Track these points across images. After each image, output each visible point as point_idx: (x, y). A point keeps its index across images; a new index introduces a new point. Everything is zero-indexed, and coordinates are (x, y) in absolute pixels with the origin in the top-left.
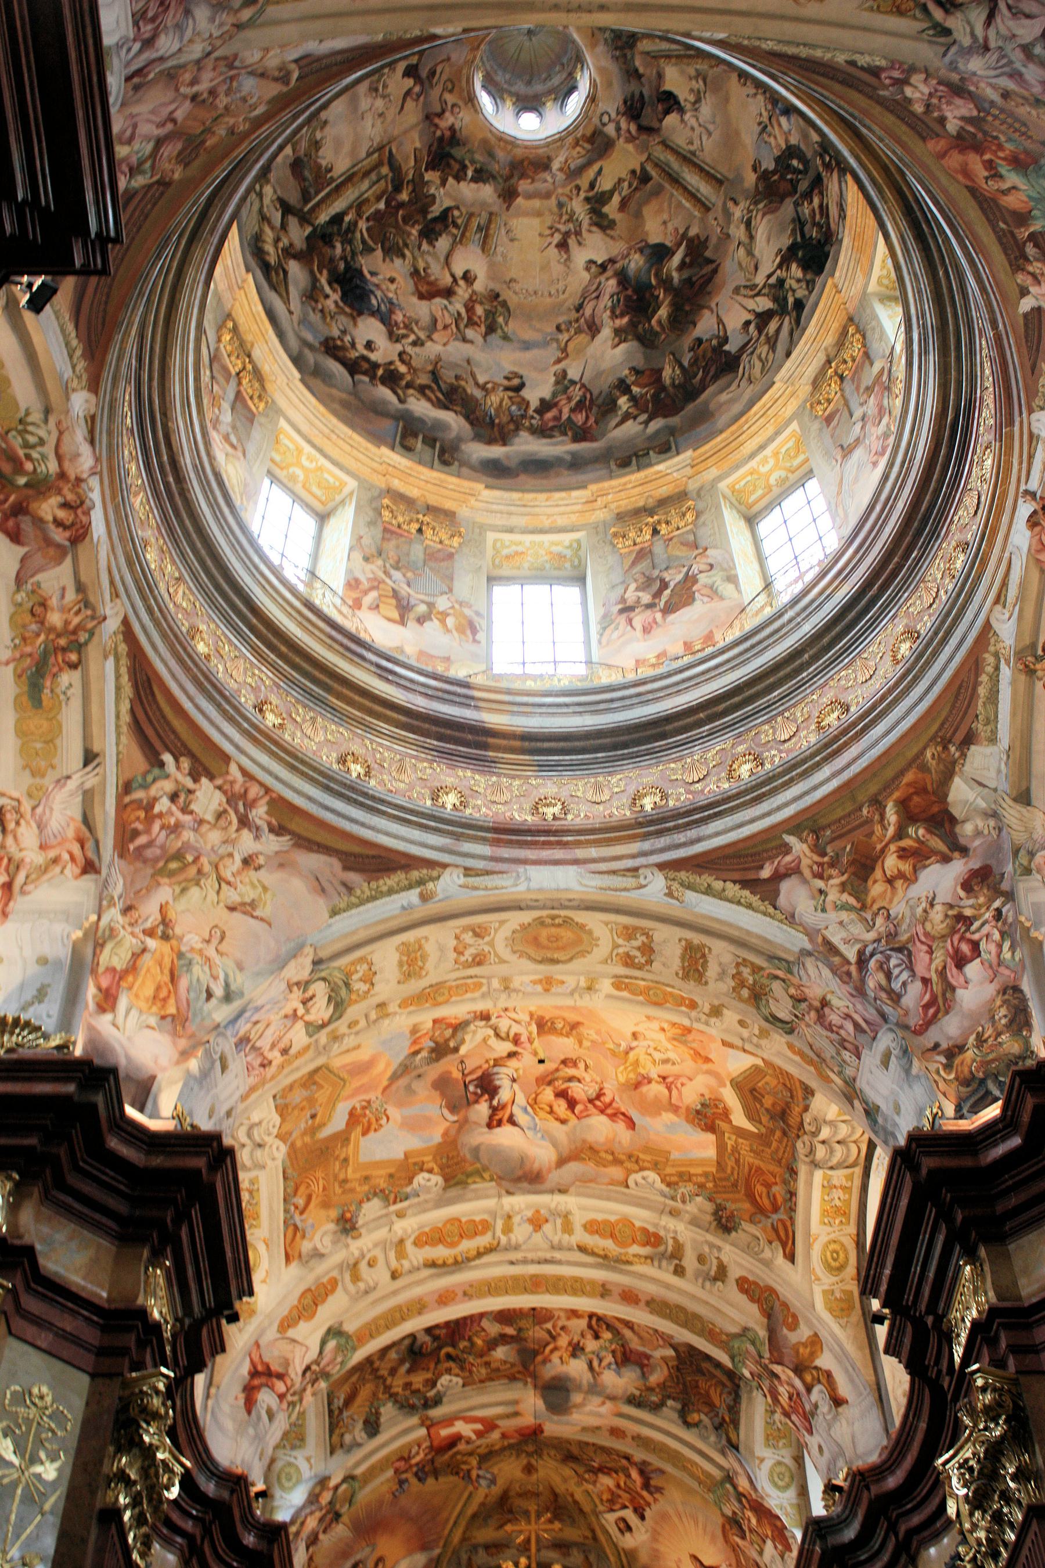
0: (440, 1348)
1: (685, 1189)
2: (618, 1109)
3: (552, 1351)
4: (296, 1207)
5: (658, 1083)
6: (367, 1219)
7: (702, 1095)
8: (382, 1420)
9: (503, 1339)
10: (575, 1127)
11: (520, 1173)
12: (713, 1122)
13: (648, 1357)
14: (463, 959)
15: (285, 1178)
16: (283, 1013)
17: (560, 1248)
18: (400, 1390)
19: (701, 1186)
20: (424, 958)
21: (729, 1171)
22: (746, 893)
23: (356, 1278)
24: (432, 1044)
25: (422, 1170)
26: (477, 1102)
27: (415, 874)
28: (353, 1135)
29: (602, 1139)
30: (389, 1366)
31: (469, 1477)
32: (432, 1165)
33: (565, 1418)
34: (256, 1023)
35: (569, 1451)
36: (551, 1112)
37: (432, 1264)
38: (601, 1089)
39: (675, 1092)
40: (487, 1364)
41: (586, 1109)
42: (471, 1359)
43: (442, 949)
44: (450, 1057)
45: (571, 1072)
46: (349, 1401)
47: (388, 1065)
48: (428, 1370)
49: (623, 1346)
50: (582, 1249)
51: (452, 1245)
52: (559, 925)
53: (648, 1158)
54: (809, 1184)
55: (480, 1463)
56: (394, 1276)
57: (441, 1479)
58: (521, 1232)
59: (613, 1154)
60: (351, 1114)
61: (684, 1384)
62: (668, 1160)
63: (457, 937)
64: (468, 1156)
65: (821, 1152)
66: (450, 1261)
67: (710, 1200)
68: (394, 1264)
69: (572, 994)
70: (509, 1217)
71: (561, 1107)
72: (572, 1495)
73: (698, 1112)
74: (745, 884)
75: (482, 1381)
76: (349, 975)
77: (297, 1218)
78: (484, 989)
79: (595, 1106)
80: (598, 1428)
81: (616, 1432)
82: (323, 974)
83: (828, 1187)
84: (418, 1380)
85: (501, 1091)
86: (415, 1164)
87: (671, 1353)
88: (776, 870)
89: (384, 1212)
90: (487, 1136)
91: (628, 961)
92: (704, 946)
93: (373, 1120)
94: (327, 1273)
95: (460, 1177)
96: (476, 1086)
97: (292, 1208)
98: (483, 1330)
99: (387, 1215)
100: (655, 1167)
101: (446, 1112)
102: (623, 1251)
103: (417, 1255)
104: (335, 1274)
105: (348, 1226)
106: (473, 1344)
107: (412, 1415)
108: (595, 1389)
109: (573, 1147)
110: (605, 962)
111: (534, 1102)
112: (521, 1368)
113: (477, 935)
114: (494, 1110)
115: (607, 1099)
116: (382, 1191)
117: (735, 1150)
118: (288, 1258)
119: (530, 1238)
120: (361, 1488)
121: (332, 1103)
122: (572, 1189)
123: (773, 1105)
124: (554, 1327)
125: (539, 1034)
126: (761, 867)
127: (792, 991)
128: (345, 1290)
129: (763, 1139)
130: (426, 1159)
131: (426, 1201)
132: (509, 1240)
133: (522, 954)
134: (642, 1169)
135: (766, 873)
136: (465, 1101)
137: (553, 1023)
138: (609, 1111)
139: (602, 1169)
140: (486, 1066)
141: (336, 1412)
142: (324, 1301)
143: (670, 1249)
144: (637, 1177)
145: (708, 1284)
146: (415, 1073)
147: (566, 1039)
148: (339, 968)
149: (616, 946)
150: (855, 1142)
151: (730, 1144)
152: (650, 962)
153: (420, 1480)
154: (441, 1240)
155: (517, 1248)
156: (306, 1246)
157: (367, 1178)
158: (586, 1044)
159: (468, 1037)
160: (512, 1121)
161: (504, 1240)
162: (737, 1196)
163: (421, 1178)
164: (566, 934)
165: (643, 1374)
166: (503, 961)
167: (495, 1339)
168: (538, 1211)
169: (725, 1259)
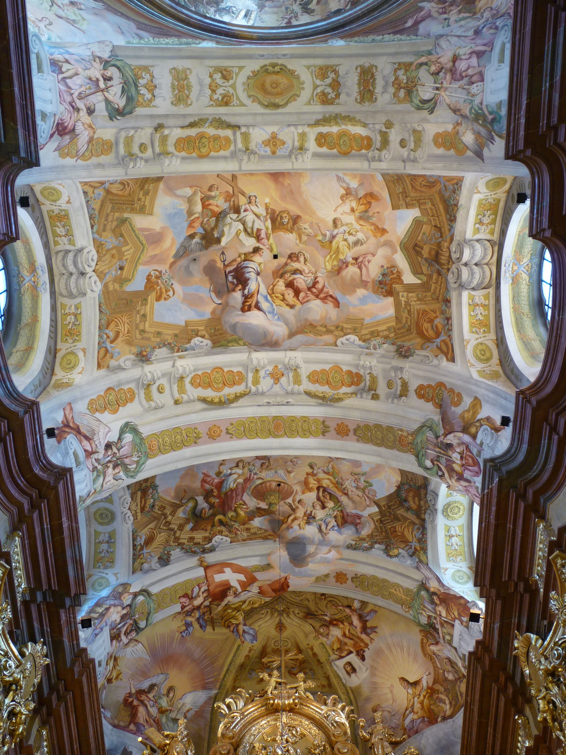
0: (214, 515)
1: (375, 341)
2: (327, 293)
3: (293, 521)
4: (108, 337)
5: (353, 264)
6: (157, 357)
7: (382, 267)
8: (172, 558)
9: (259, 512)
10: (300, 310)
11: (264, 342)
12: (391, 288)
13: (359, 517)
14: (215, 97)
15: (100, 311)
16: (88, 73)
17: (292, 393)
18: (185, 541)
19: (386, 337)
20: (189, 87)
21: (404, 321)
22: (398, 36)
23: (149, 398)
25: (197, 335)
26: (234, 290)
27: (184, 40)
29: (318, 318)
30: (178, 522)
31: (238, 631)
32: (203, 333)
33: (303, 569)
34: (67, 61)
35: (308, 608)
36: (284, 300)
37: (204, 400)
38: (316, 278)
40: (248, 529)
41: (307, 296)
42: (236, 525)
43: (201, 84)
44: (215, 247)
45: (296, 265)
46: (149, 541)
47: (173, 243)
48: (206, 530)
49: (342, 511)
50: (308, 393)
51: (218, 390)
52: (278, 73)
53: (349, 326)
54: (460, 304)
55: (245, 619)
56: (177, 402)
57: (217, 630)
58: (266, 384)
59: (326, 326)
60: (149, 277)
61: (386, 531)
62: (362, 325)
63: (211, 76)
64: (229, 330)
65: (465, 274)
66: (216, 400)
67: (393, 344)
68: (177, 396)
69: (290, 156)
70: (257, 371)
71: (290, 295)
72: (312, 649)
73: (380, 282)
74: (395, 33)
75: (244, 540)
76: (137, 77)
77: (108, 345)
78: (232, 147)
79: (313, 293)
80: (327, 576)
81: (340, 577)
82: (118, 63)
83: (473, 305)
84: (199, 536)
85: (250, 282)
86: (193, 330)
87: (375, 509)
88: (416, 20)
90: (241, 317)
91: (325, 100)
92: (372, 66)
93: (164, 290)
94: (128, 382)
95: (223, 342)
96: (234, 277)
97: (105, 336)
98: (245, 504)
100: (355, 331)
102: (335, 392)
103: (194, 392)
104: (133, 386)
105: (144, 359)
106: (238, 514)
107: (194, 556)
108: (323, 542)
109: (299, 325)
110: (309, 103)
111: (272, 292)
112: (271, 533)
113: (224, 77)
114: (246, 298)
117: (407, 303)
118: (99, 366)
119: (271, 388)
120: (157, 611)
121: (136, 262)
123: (430, 253)
124: (294, 501)
125: (273, 229)
126: (406, 22)
127: (433, 68)
128: (140, 403)
129: (425, 286)
130: (200, 328)
132: (258, 389)
133: (255, 99)
134: (346, 334)
135: (410, 23)
136: (226, 289)
138: (322, 296)
139: (319, 337)
141: (139, 547)
142: (125, 405)
143: (368, 383)
144: (343, 339)
145: (396, 401)
148: (130, 66)
149: (316, 87)
150: (487, 264)
151: (403, 300)
152: (338, 96)
153: (201, 627)
154: (209, 385)
155: (263, 394)
156: (113, 363)
157: (159, 333)
158: (304, 238)
159: (226, 229)
160: (258, 307)
161: (253, 389)
162: (411, 336)
163: (196, 340)
164: (283, 80)
165: (357, 530)
166: (242, 105)
167: (253, 511)
168: (276, 366)
169: (406, 376)
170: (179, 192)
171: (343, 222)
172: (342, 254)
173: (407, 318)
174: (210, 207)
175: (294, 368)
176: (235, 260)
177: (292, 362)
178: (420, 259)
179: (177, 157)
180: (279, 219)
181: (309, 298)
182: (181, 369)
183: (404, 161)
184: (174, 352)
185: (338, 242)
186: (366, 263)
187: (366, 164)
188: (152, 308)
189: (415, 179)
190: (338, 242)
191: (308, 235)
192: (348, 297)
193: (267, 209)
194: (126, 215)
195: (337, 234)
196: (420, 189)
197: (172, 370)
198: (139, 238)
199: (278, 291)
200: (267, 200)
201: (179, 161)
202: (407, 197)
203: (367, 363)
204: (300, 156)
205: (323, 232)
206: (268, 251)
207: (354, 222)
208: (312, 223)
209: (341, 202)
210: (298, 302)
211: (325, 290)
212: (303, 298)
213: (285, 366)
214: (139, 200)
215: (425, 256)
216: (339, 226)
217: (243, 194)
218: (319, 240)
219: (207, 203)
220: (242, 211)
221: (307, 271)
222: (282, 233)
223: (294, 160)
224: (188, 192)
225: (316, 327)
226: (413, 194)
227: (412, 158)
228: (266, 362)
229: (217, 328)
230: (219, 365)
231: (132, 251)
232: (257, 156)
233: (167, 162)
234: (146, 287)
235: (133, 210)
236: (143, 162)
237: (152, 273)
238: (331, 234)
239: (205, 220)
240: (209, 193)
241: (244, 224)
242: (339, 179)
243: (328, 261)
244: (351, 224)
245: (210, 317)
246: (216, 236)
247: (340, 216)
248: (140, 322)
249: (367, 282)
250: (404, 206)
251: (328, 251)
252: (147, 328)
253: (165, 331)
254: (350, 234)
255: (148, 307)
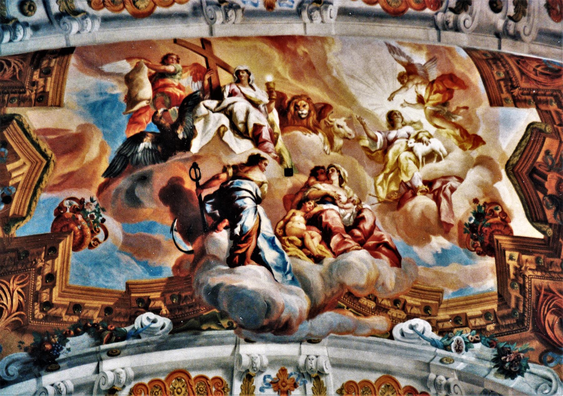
2: (380, 238)
5: (424, 193)
6: (70, 354)
7: (476, 201)
11: (265, 322)
19: (480, 330)
21: (513, 305)
24: (155, 129)
26: (215, 228)
28: (61, 245)
29: (363, 282)
32: (159, 304)
36: (303, 246)
38: (360, 211)
39: (444, 203)
44: (180, 156)
45: (324, 188)
47: (103, 151)
59: (375, 299)
60: (60, 211)
62: (440, 301)
67: (491, 345)
69: (298, 13)
73: (472, 228)
79: (354, 237)
85: (244, 215)
86: (140, 300)
89: (94, 349)
90: (228, 275)
93: (88, 232)
99: (96, 353)
101: (178, 237)
115: (367, 226)
116: (96, 326)
117: (519, 272)
122: (325, 341)
130: (153, 295)
131: (147, 343)
134: (410, 317)
136: (200, 226)
137: (297, 108)
138: (371, 243)
139: (362, 319)
140: (224, 176)
144: (404, 326)
146: (139, 172)
147: (314, 135)
151: (512, 264)
158: (339, 142)
159: (199, 125)
163: (144, 318)
168: (283, 371)
170: (107, 68)
171: (406, 119)
172: (406, 173)
173: (517, 299)
174: (170, 90)
175: (315, 374)
176: (216, 177)
177: (312, 364)
178: (541, 196)
179: (94, 17)
180: (292, 108)
181: (348, 246)
182: (111, 377)
183: (498, 35)
184: (101, 343)
185: (397, 153)
186: (448, 192)
187: (433, 32)
188: (66, 262)
189: (524, 62)
190: (397, 153)
191: (345, 138)
192: (415, 249)
193: (270, 91)
194: (9, 110)
195: (396, 138)
196: (535, 78)
197: (94, 378)
198: (37, 147)
199: (295, 231)
200: (269, 78)
201: (97, 24)
202: (513, 87)
203: (442, 377)
204: (316, 13)
205: (371, 134)
206: (276, 163)
207: (424, 121)
208: (351, 117)
209: (398, 85)
210: (328, 252)
211: (376, 233)
212: (338, 245)
213: (298, 369)
214: (34, 83)
215: (550, 192)
216: (399, 125)
217: (226, 68)
218: (365, 148)
219: (161, 83)
220: (226, 94)
221: (344, 199)
222: (299, 133)
223: (307, 20)
224: (125, 66)
225: (358, 298)
226: (524, 85)
227: (511, 31)
228: (266, 362)
229: (183, 295)
230: (181, 367)
231: (25, 169)
232: (239, 12)
233: (75, 26)
234: (53, 227)
235: (24, 102)
236: (29, 31)
237: (66, 203)
238: (386, 138)
239: (160, 111)
240: (163, 67)
241: (230, 115)
242: (392, 49)
243: (381, 184)
244: (420, 123)
245: (171, 274)
246: (181, 136)
247: (398, 108)
248: (43, 288)
249: (450, 226)
250: (511, 101)
251: (382, 166)
252: (56, 299)
253: (88, 303)
254: (418, 139)
255: (58, 262)
